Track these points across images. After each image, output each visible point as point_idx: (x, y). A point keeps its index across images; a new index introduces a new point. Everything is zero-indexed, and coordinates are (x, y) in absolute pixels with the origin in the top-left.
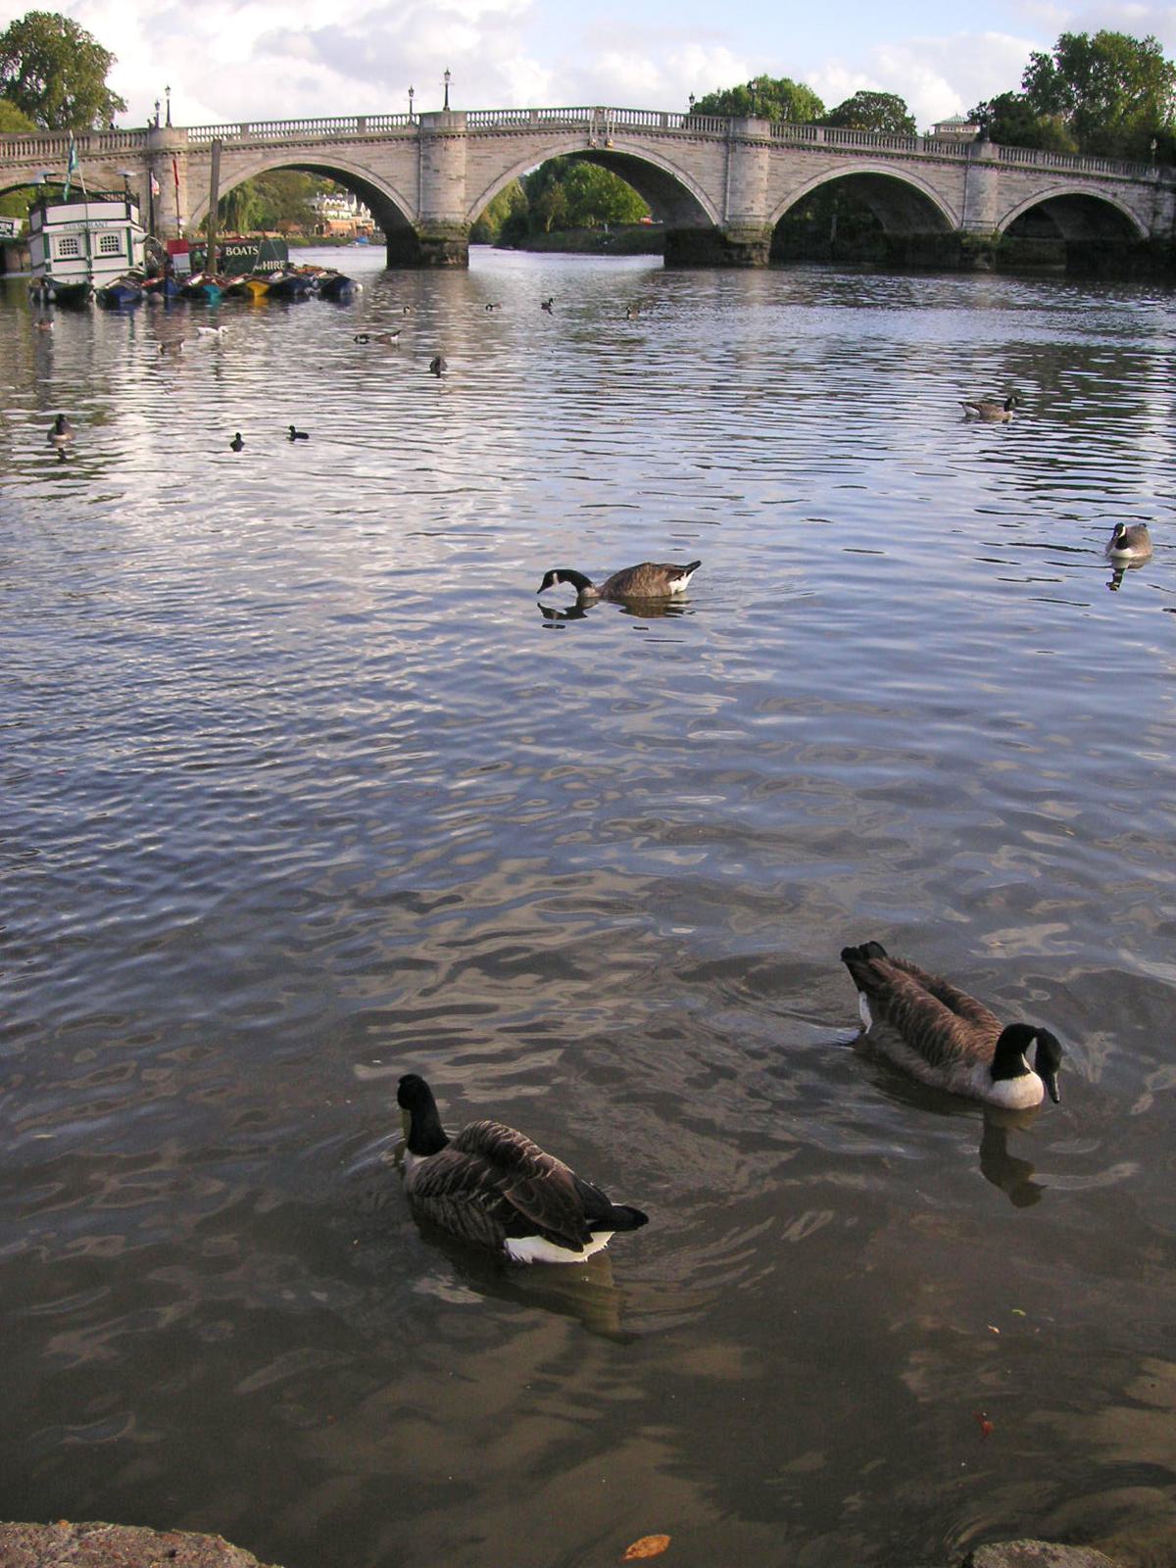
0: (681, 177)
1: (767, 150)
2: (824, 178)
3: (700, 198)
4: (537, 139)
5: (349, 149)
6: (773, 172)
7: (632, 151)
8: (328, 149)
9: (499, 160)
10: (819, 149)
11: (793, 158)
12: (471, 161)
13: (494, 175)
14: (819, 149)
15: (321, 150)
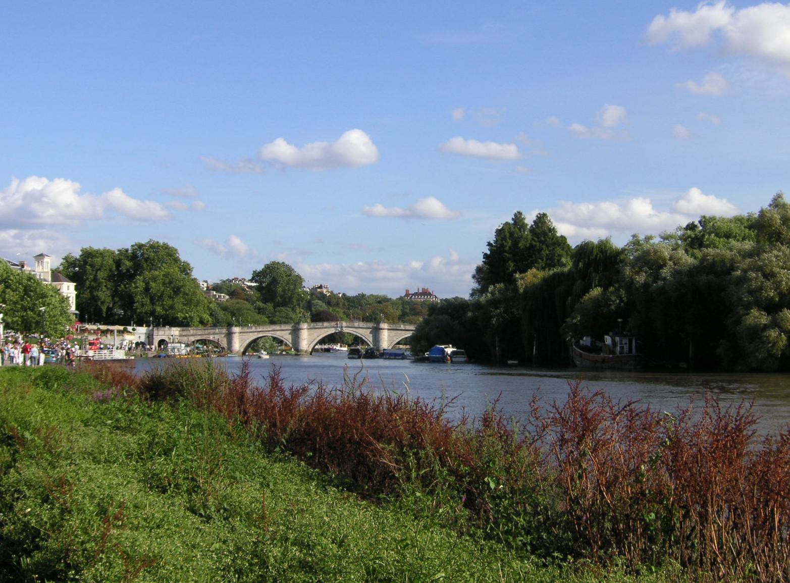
0: (364, 338)
1: (386, 331)
2: (403, 337)
3: (369, 343)
4: (326, 329)
5: (278, 332)
6: (389, 336)
7: (351, 332)
8: (273, 332)
9: (316, 335)
10: (402, 330)
11: (395, 332)
12: (309, 335)
13: (314, 338)
14: (402, 330)
15: (271, 332)
